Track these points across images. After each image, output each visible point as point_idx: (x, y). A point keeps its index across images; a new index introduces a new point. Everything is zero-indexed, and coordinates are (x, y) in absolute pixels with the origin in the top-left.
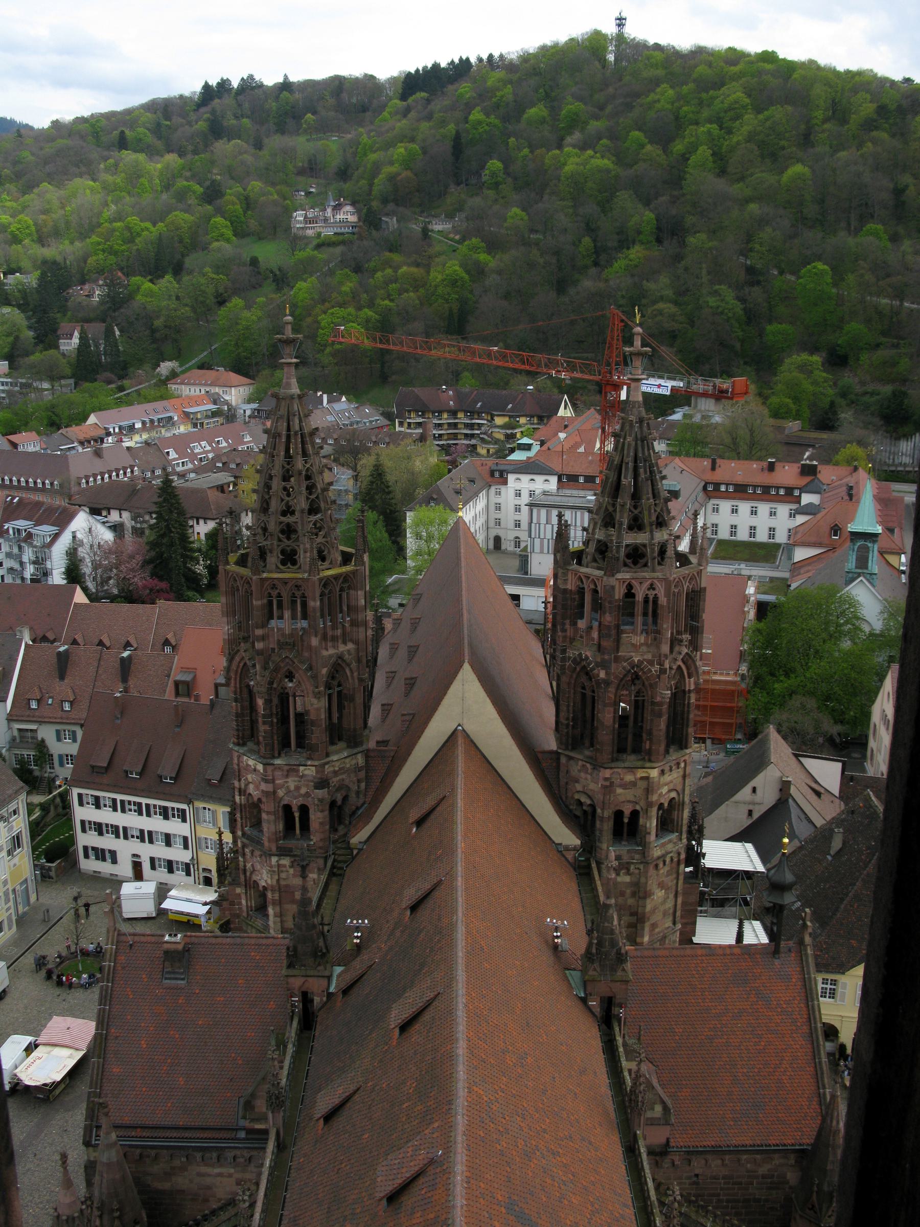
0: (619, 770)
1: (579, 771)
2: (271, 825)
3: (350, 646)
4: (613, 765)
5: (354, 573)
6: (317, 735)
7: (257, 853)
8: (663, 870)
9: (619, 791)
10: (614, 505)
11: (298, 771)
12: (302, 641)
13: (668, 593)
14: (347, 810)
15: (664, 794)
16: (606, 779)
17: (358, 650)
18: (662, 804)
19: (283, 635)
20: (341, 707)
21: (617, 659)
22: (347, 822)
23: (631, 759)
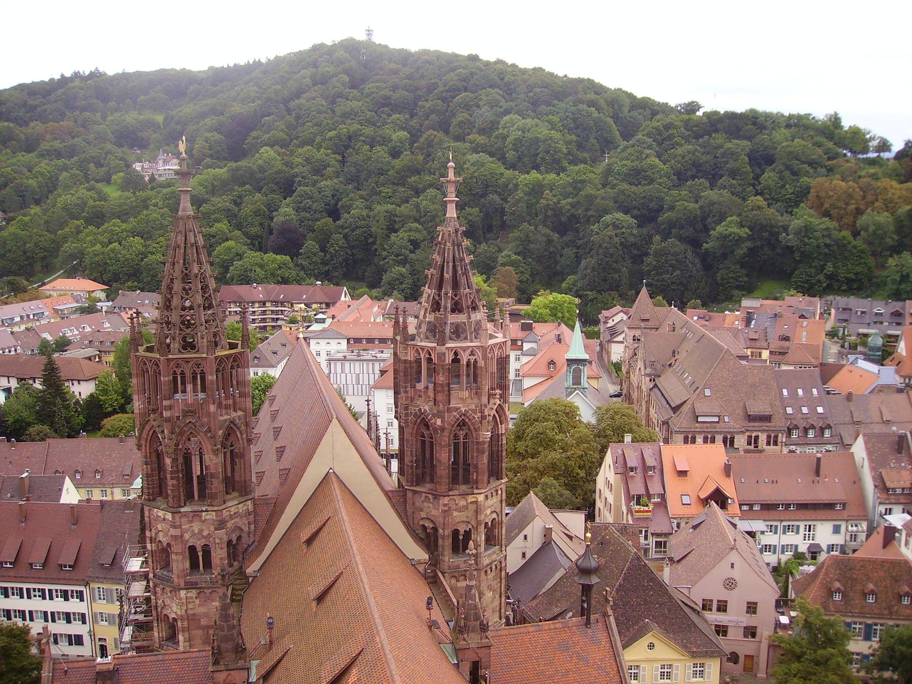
0: (455, 497)
1: (423, 502)
2: (179, 563)
3: (240, 413)
4: (450, 493)
5: (241, 354)
6: (216, 485)
7: (168, 589)
8: (491, 576)
9: (455, 514)
10: (439, 295)
11: (201, 517)
12: (202, 409)
13: (485, 357)
14: (240, 549)
15: (488, 516)
16: (445, 505)
17: (245, 416)
18: (486, 523)
19: (187, 405)
20: (233, 463)
21: (449, 410)
22: (241, 559)
23: (463, 488)
